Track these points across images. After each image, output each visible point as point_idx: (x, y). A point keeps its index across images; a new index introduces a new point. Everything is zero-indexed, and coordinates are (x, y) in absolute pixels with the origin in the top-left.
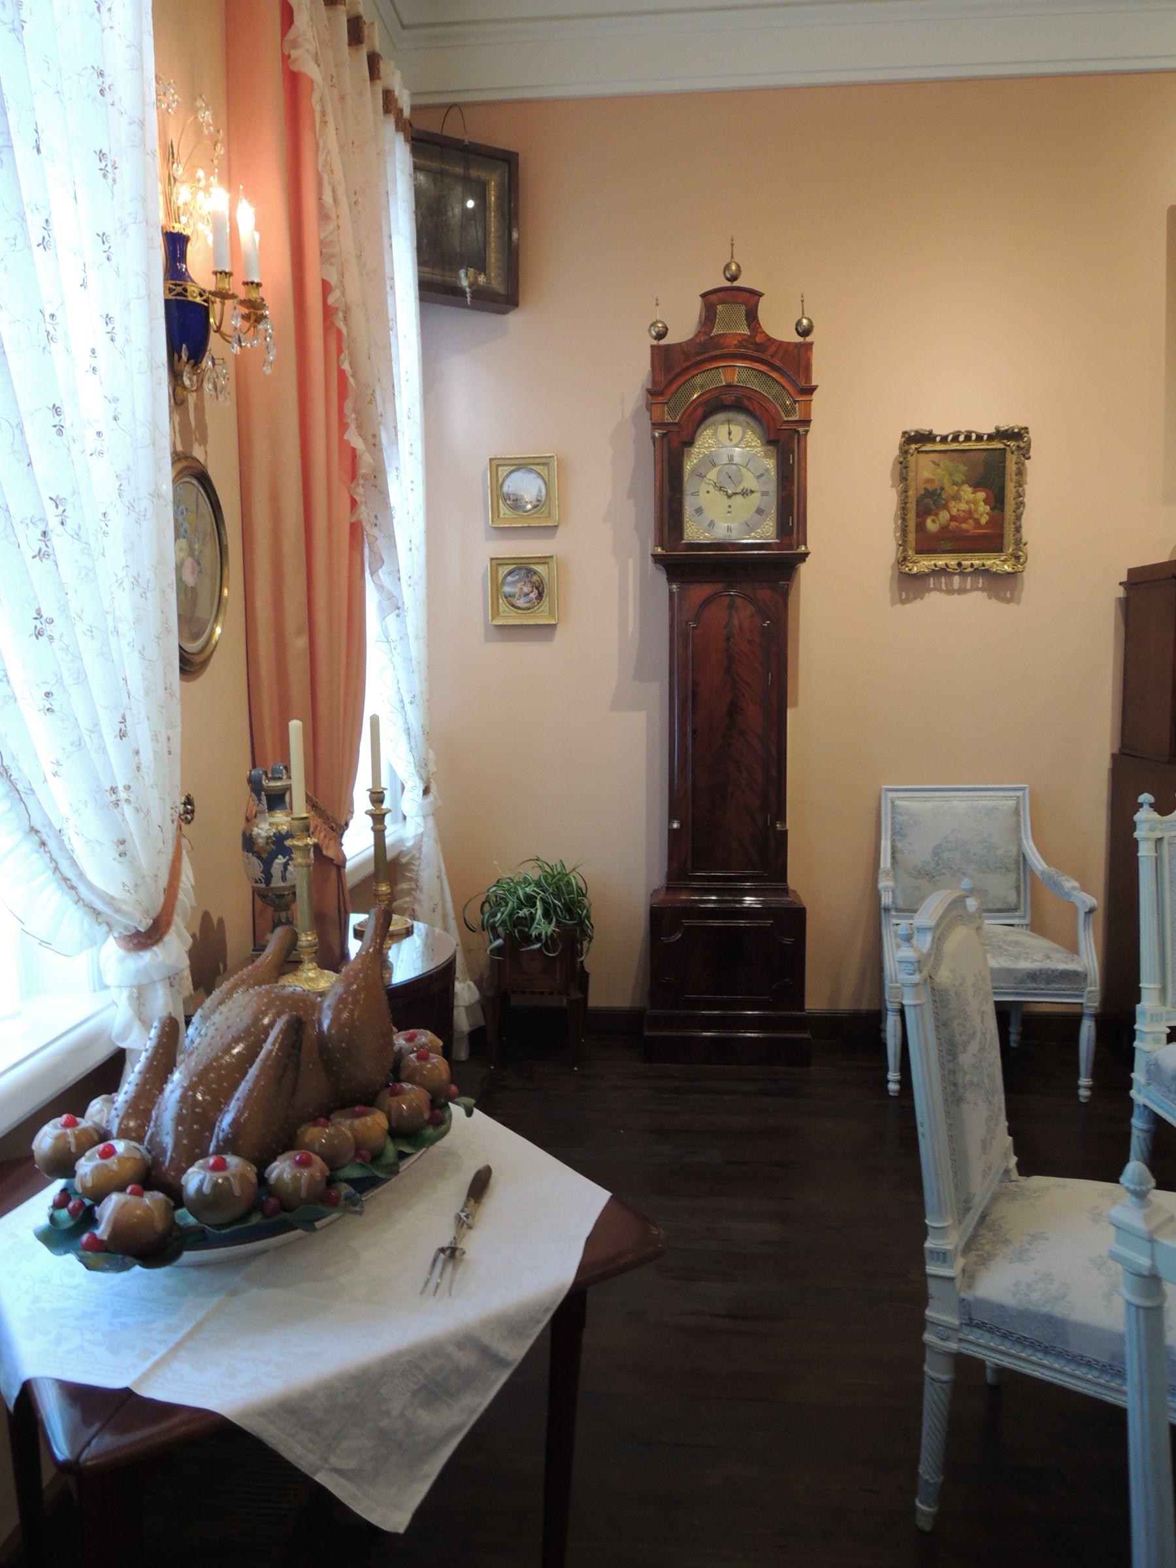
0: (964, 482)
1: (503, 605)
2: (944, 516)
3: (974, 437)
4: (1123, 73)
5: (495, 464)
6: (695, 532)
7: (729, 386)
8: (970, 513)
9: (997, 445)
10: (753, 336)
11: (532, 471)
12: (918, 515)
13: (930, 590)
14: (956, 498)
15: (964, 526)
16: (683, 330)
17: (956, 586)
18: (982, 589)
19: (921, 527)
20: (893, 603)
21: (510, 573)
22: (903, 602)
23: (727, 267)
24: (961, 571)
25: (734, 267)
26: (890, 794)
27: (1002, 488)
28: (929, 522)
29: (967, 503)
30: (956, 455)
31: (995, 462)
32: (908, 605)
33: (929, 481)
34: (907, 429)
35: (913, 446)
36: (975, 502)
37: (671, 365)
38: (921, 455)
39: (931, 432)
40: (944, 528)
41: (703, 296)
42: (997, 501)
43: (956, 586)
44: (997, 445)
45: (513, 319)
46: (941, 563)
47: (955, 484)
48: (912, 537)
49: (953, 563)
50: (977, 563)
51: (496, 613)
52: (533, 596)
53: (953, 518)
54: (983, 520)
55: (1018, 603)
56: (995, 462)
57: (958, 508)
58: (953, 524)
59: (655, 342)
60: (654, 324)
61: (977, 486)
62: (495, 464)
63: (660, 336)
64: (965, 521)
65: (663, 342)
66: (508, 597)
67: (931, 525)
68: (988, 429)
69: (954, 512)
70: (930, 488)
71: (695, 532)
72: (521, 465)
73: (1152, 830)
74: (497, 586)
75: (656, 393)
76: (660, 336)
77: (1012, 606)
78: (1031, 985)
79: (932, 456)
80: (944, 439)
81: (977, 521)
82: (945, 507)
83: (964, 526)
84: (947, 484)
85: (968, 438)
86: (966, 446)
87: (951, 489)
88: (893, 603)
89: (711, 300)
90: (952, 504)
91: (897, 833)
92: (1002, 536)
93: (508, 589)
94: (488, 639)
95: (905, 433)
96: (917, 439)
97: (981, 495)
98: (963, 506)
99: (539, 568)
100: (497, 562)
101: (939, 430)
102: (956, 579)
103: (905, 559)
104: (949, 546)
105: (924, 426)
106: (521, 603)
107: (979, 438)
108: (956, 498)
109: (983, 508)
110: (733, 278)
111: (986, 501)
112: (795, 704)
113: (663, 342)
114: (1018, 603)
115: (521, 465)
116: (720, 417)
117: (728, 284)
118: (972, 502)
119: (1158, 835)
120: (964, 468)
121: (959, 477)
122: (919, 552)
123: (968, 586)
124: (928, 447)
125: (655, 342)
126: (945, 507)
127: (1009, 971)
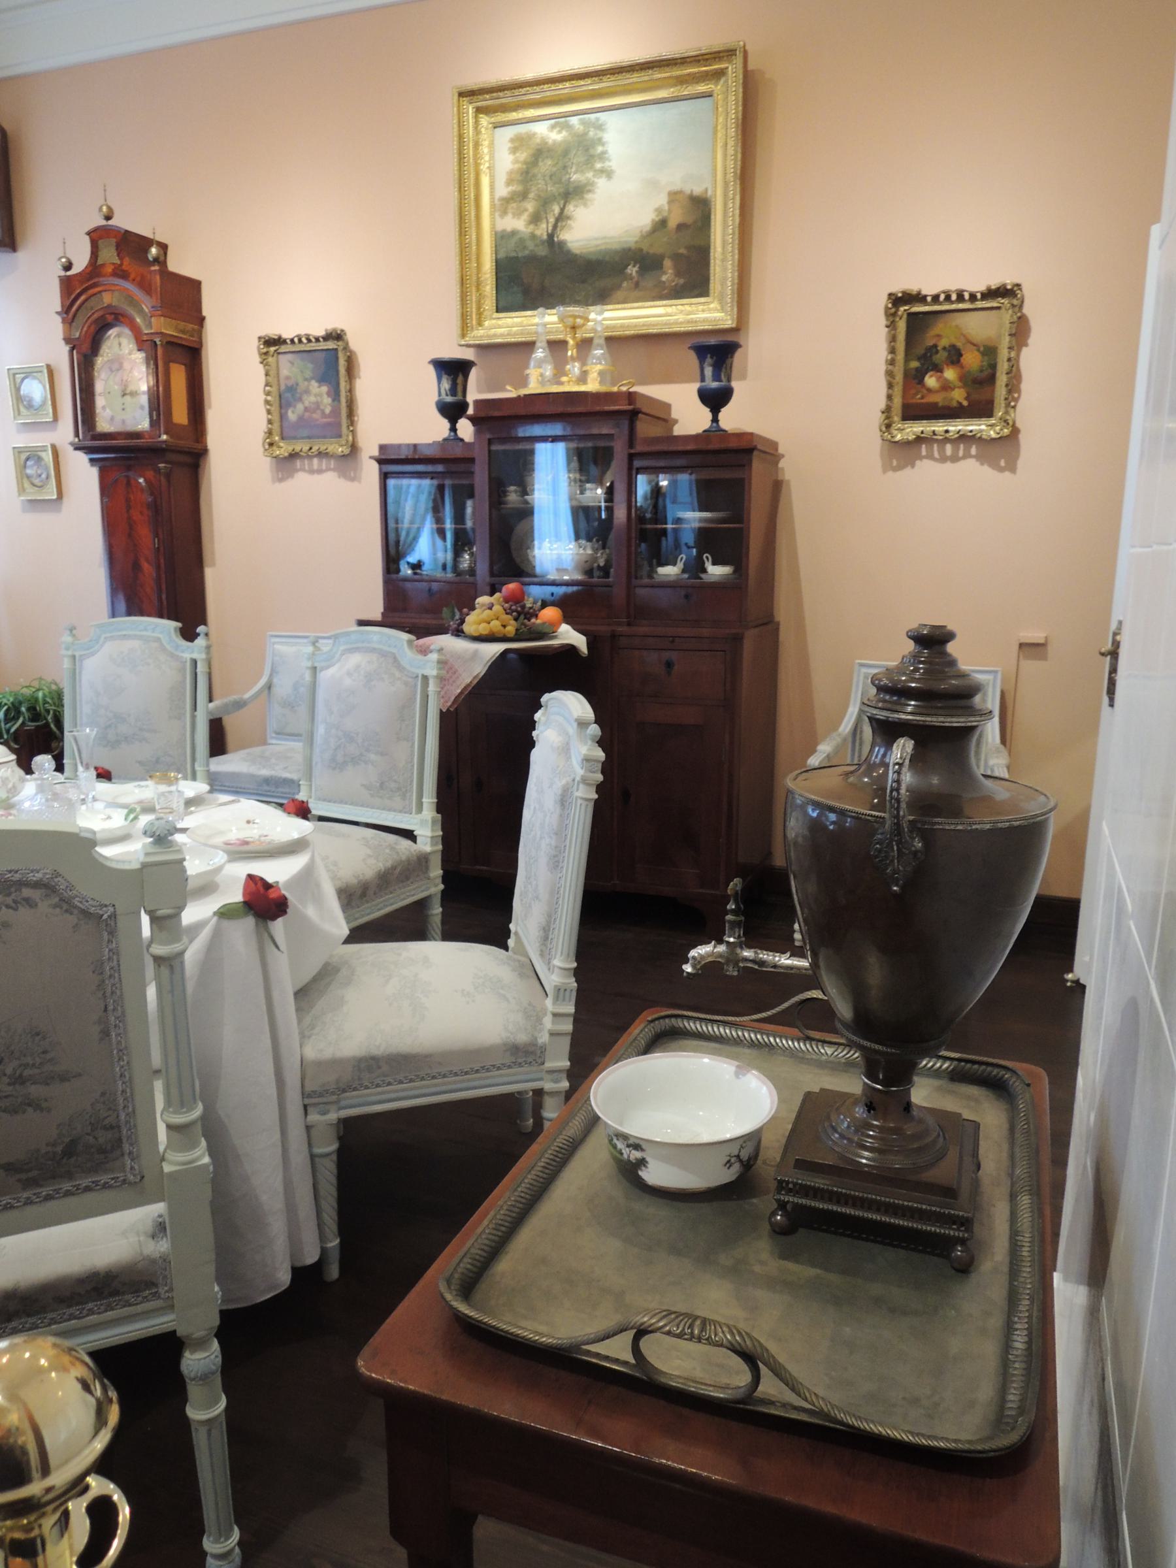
0: (312, 378)
1: (27, 485)
2: (300, 407)
3: (304, 340)
4: (341, 15)
5: (12, 374)
6: (105, 423)
7: (109, 306)
8: (317, 405)
9: (331, 345)
10: (121, 265)
11: (35, 378)
12: (281, 407)
13: (297, 471)
14: (307, 392)
15: (314, 416)
16: (81, 263)
17: (315, 467)
18: (333, 470)
19: (282, 417)
20: (274, 482)
21: (27, 459)
22: (281, 480)
23: (100, 209)
24: (321, 454)
25: (104, 209)
26: (274, 640)
27: (338, 384)
28: (290, 413)
29: (316, 395)
30: (305, 355)
31: (332, 358)
32: (284, 485)
33: (288, 378)
34: (263, 334)
35: (272, 349)
36: (320, 395)
37: (76, 290)
38: (280, 356)
39: (280, 337)
40: (301, 418)
41: (89, 233)
42: (335, 394)
43: (315, 467)
44: (331, 345)
45: (21, 255)
46: (298, 449)
47: (306, 379)
48: (276, 427)
49: (306, 448)
50: (323, 448)
51: (22, 490)
52: (44, 476)
53: (306, 409)
54: (328, 410)
55: (360, 482)
56: (332, 358)
57: (309, 400)
58: (307, 414)
59: (63, 273)
60: (60, 259)
61: (322, 380)
62: (12, 374)
63: (68, 267)
64: (314, 412)
65: (69, 273)
66: (28, 477)
67: (292, 416)
68: (321, 333)
69: (307, 403)
70: (290, 383)
71: (105, 423)
72: (28, 374)
73: (67, 649)
74: (21, 467)
75: (69, 312)
76: (68, 267)
77: (356, 484)
78: (266, 788)
79: (289, 356)
80: (292, 341)
81: (323, 412)
82: (300, 399)
83: (314, 416)
84: (300, 381)
85: (309, 341)
86: (309, 347)
87: (303, 385)
88: (274, 482)
89: (97, 236)
90: (305, 397)
91: (273, 672)
92: (339, 425)
93: (29, 471)
94: (24, 511)
95: (260, 338)
96: (272, 343)
97: (324, 389)
98: (312, 399)
99: (43, 455)
100: (18, 451)
101: (287, 335)
102: (315, 461)
103: (271, 444)
104: (305, 433)
105: (273, 331)
106: (37, 481)
107: (317, 340)
108: (307, 392)
109: (327, 400)
110: (108, 218)
111: (328, 394)
112: (213, 565)
113: (69, 273)
114: (360, 482)
115: (28, 374)
116: (112, 332)
117: (104, 223)
118: (318, 394)
119: (70, 653)
120: (310, 366)
121: (308, 374)
122: (282, 438)
123: (324, 467)
124: (283, 348)
125: (63, 273)
126: (300, 399)
127: (252, 776)
